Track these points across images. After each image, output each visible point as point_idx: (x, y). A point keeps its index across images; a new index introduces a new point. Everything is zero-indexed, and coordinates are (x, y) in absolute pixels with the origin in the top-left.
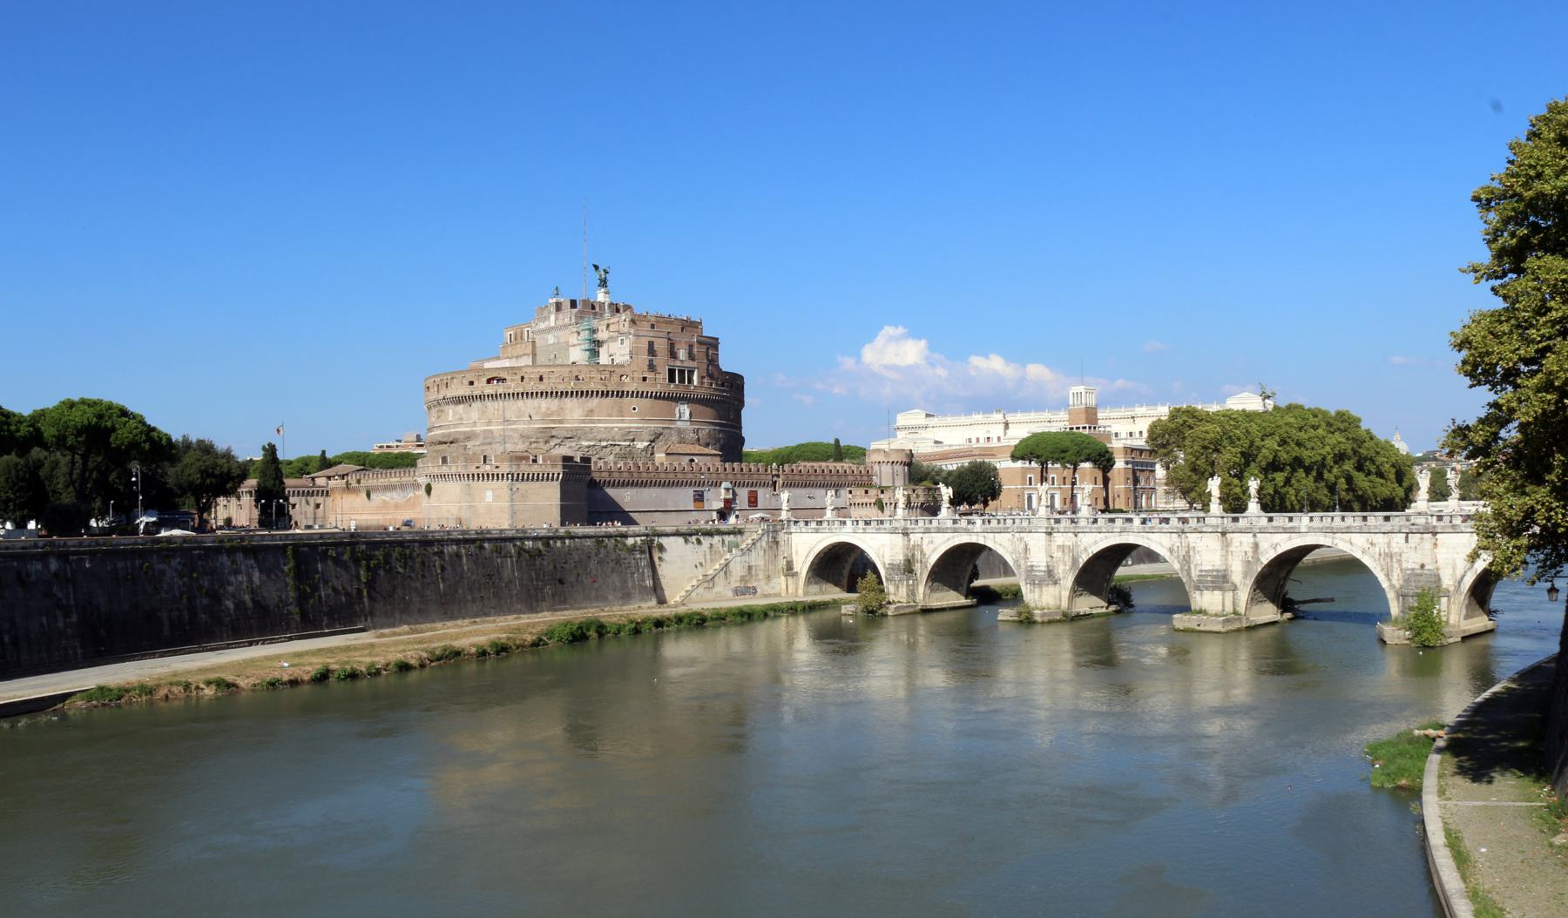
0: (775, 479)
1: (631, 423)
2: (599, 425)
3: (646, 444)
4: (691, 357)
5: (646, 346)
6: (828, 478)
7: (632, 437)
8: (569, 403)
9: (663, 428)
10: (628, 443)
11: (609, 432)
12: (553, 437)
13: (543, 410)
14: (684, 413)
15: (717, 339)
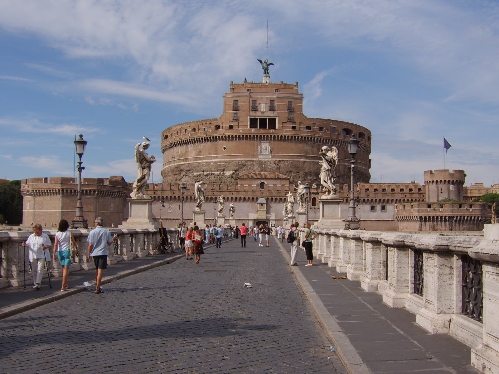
0: (313, 196)
1: (222, 158)
2: (204, 161)
3: (231, 172)
4: (272, 109)
5: (232, 104)
6: (372, 196)
7: (223, 168)
8: (191, 147)
9: (246, 161)
10: (219, 173)
11: (208, 165)
12: (182, 170)
13: (179, 153)
14: (266, 149)
15: (302, 94)
